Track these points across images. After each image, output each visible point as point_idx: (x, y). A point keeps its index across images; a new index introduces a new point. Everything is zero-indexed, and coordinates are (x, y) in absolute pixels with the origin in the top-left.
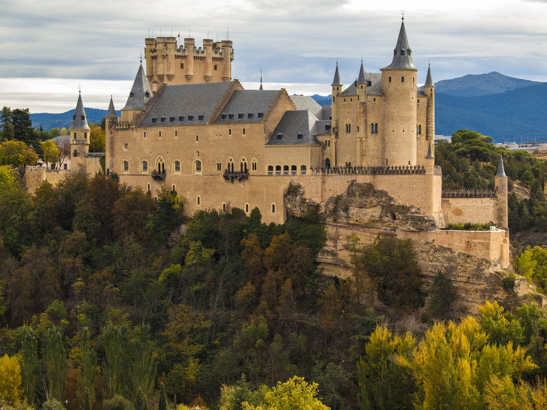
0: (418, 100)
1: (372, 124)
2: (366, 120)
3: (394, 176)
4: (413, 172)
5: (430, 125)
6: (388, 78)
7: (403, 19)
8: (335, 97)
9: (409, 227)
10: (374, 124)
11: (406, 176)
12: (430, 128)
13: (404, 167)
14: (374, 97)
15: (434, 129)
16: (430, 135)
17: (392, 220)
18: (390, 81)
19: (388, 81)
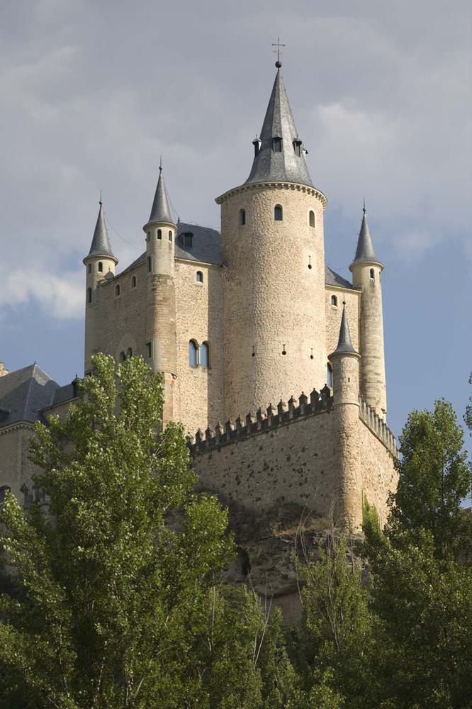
0: (334, 298)
1: (193, 342)
2: (173, 325)
3: (244, 444)
4: (296, 412)
5: (370, 368)
6: (238, 215)
7: (278, 65)
8: (95, 287)
9: (283, 571)
10: (200, 342)
11: (280, 433)
12: (371, 376)
13: (269, 409)
14: (200, 269)
15: (382, 378)
16: (371, 393)
17: (239, 576)
18: (244, 223)
19: (237, 222)
